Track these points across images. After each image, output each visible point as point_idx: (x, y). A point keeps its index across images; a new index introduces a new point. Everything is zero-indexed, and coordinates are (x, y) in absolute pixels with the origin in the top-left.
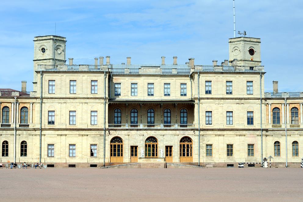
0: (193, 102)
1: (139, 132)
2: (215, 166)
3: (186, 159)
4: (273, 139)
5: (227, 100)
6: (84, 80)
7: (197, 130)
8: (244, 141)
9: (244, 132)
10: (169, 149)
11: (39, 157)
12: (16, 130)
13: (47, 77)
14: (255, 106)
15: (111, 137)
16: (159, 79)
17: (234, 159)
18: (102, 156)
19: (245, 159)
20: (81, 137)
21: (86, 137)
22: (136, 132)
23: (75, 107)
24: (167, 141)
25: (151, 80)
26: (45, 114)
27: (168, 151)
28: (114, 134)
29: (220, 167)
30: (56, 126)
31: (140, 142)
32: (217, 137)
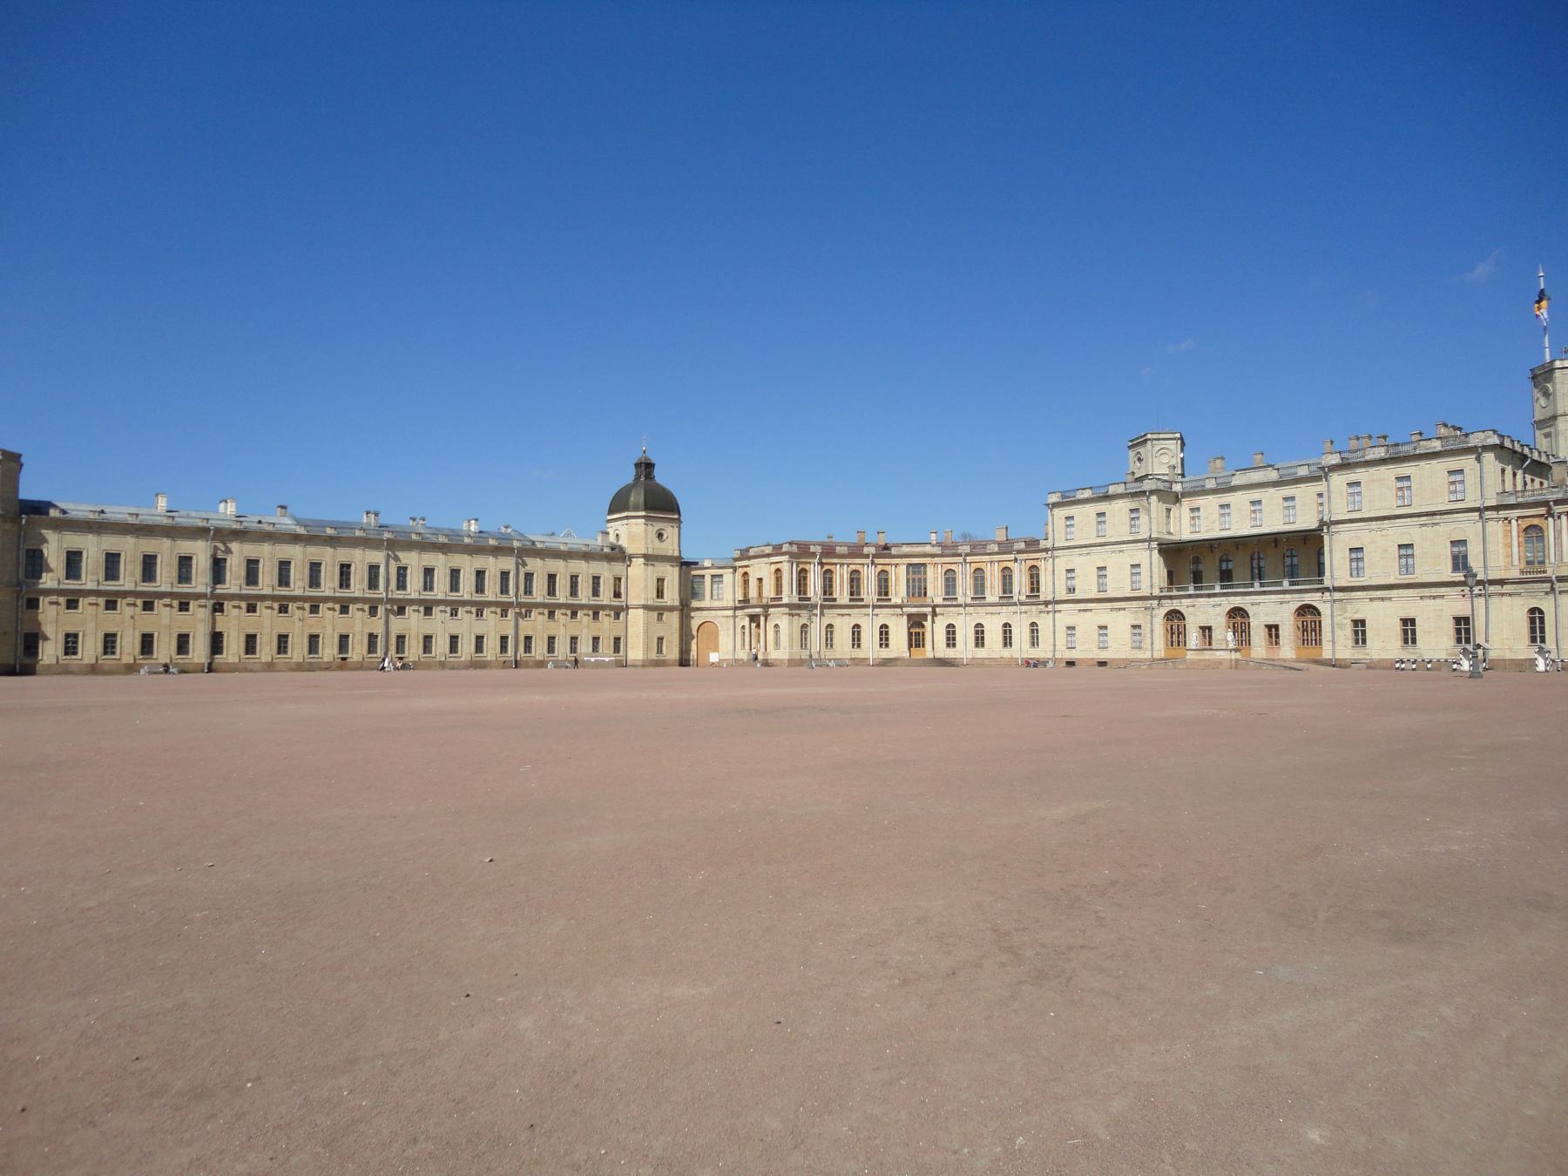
0: (1319, 532)
1: (1212, 599)
2: (1371, 666)
3: (1311, 652)
4: (1522, 603)
5: (1397, 521)
6: (1118, 510)
7: (1327, 589)
8: (1442, 610)
9: (1442, 590)
10: (1273, 630)
11: (1052, 648)
12: (1022, 604)
13: (1061, 513)
14: (1467, 527)
15: (1163, 611)
16: (1272, 490)
17: (1418, 651)
18: (1149, 647)
19: (1447, 650)
20: (1115, 613)
21: (1122, 612)
22: (1207, 599)
23: (1104, 560)
24: (1267, 615)
25: (1255, 495)
26: (1061, 576)
27: (1536, 630)
28: (1168, 606)
29: (1384, 668)
30: (1078, 595)
31: (1216, 619)
32: (1375, 603)
